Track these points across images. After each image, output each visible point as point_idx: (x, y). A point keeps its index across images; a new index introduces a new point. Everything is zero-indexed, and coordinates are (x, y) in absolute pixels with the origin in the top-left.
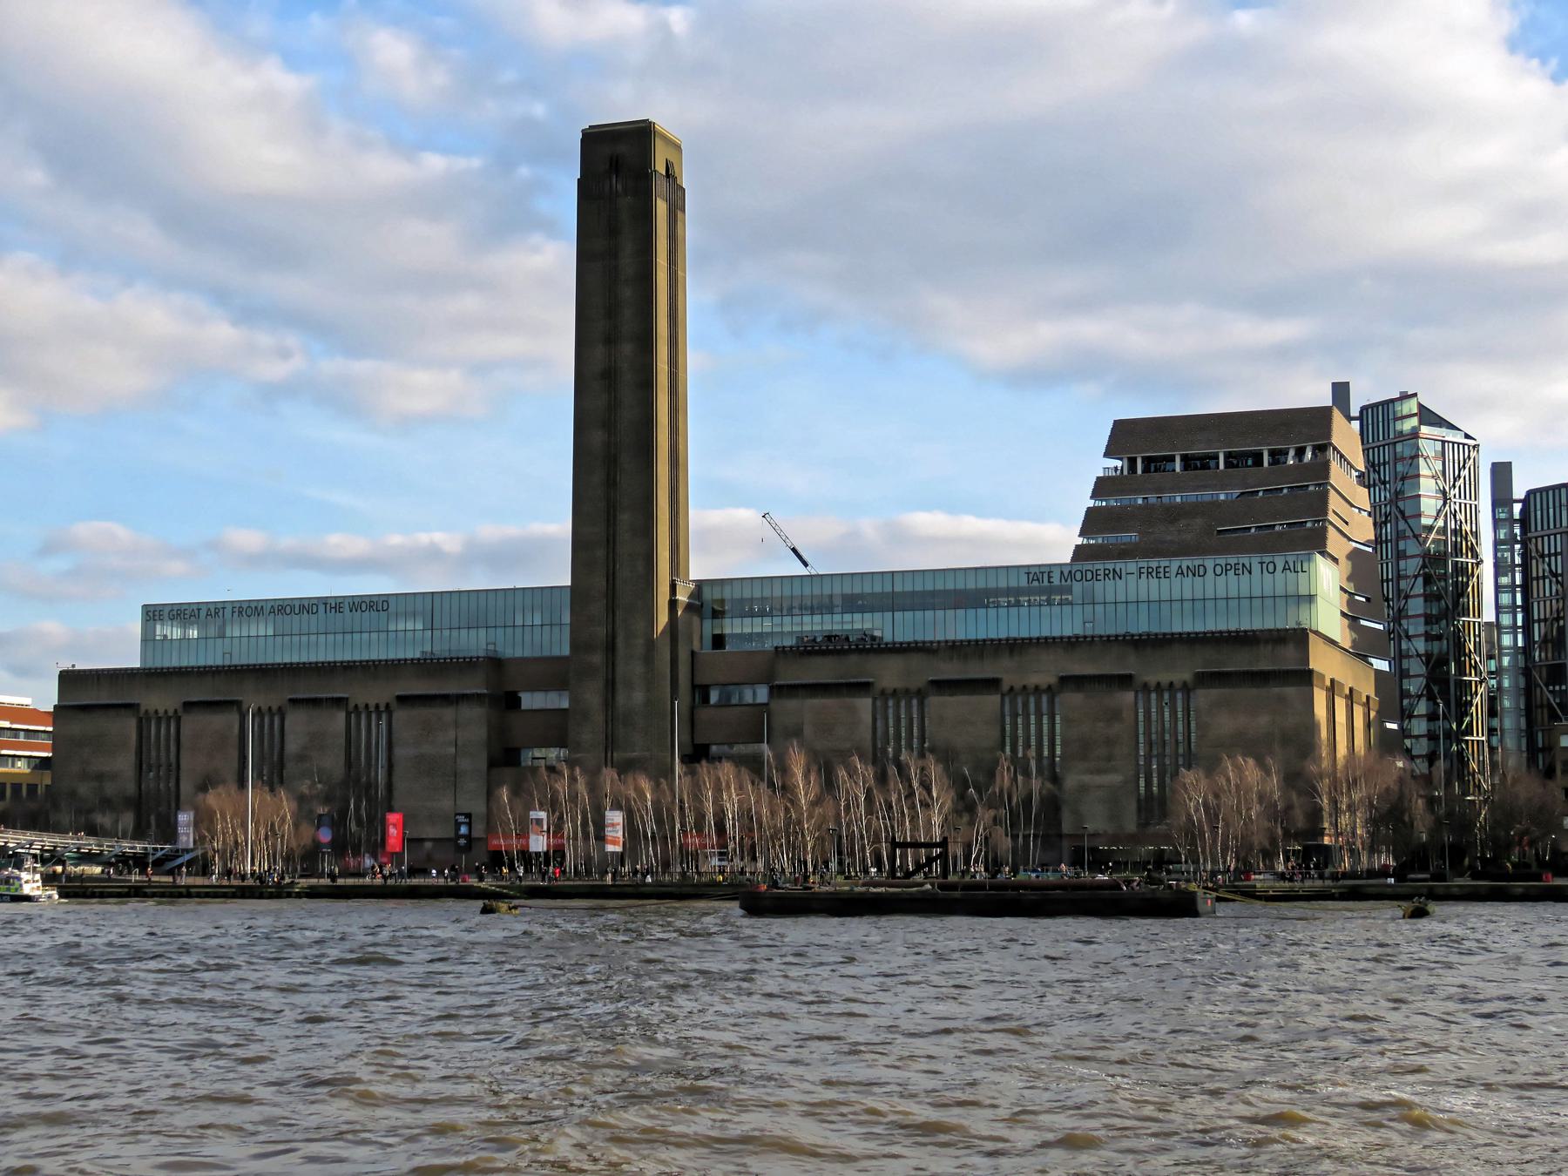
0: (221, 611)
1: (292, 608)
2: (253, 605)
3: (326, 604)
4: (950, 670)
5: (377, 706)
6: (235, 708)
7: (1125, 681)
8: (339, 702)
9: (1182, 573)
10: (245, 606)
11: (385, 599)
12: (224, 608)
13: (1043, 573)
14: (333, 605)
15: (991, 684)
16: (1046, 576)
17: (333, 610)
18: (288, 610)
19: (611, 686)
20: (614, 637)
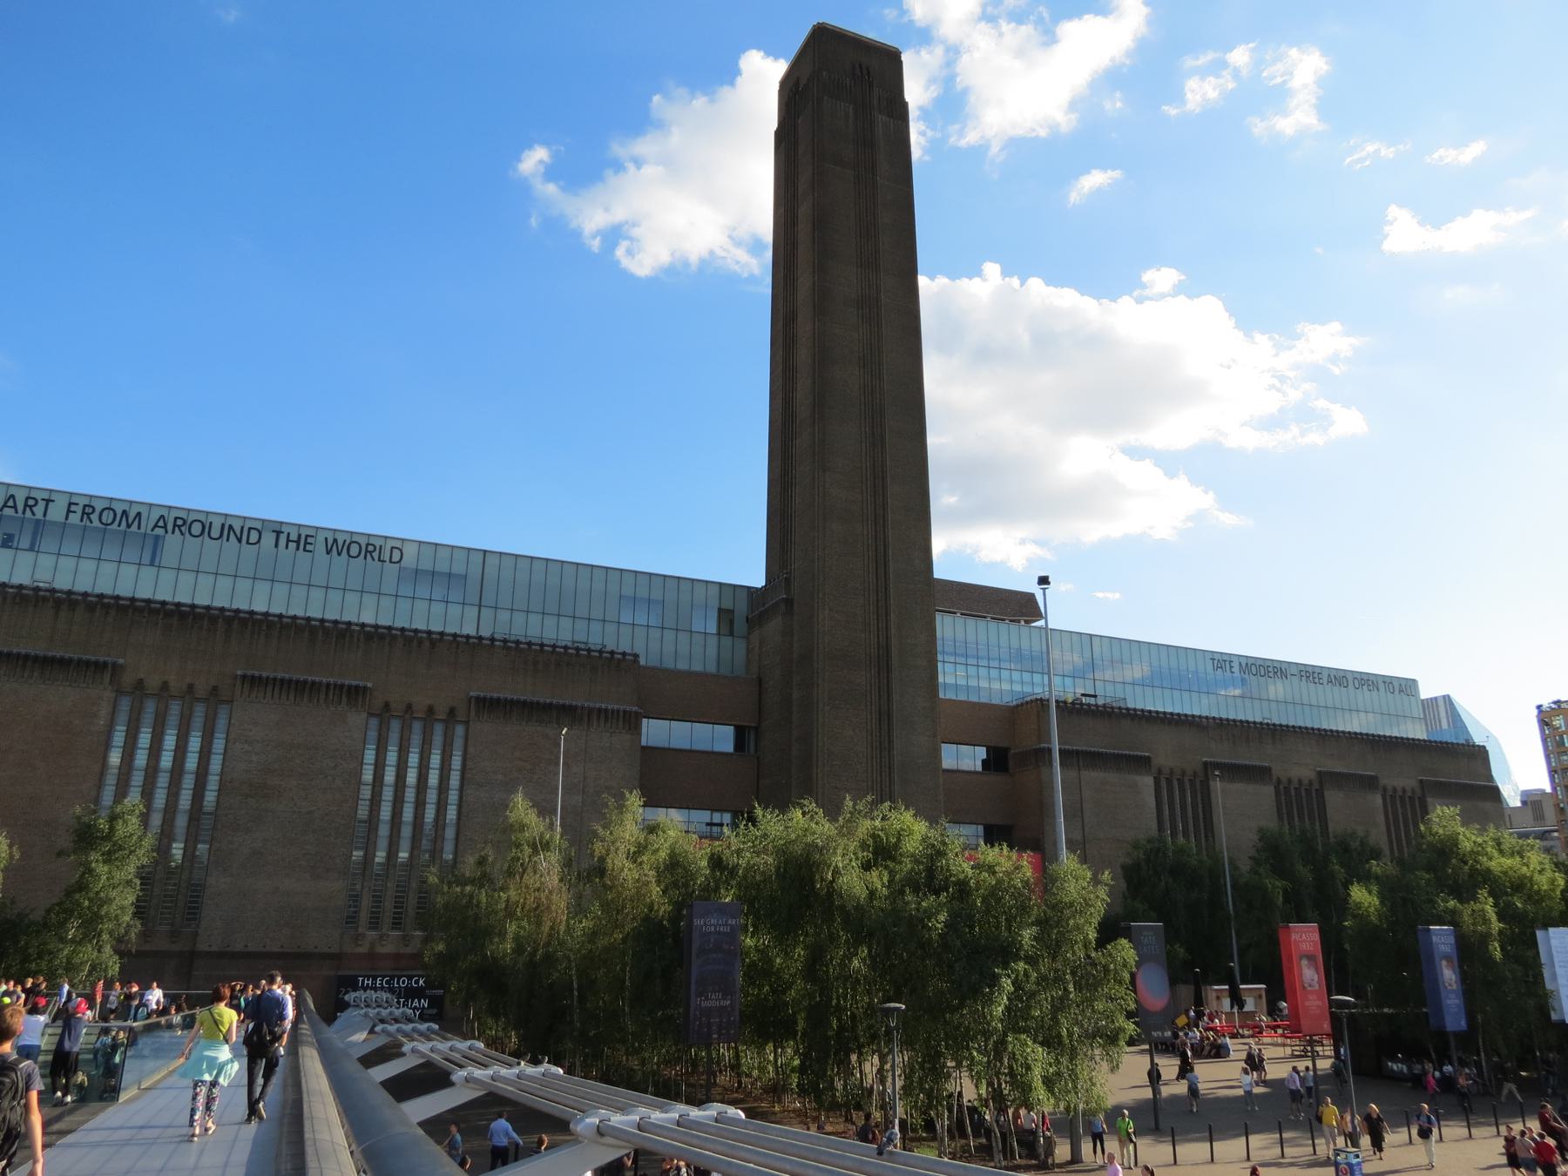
0: (42, 505)
1: (206, 529)
2: (119, 509)
3: (278, 533)
4: (1222, 752)
5: (431, 710)
6: (107, 677)
7: (1370, 783)
8: (355, 694)
9: (1331, 682)
10: (99, 506)
11: (398, 544)
12: (48, 501)
13: (1225, 661)
14: (294, 537)
15: (1257, 774)
16: (1227, 663)
17: (292, 546)
18: (196, 529)
19: (885, 717)
20: (888, 648)
